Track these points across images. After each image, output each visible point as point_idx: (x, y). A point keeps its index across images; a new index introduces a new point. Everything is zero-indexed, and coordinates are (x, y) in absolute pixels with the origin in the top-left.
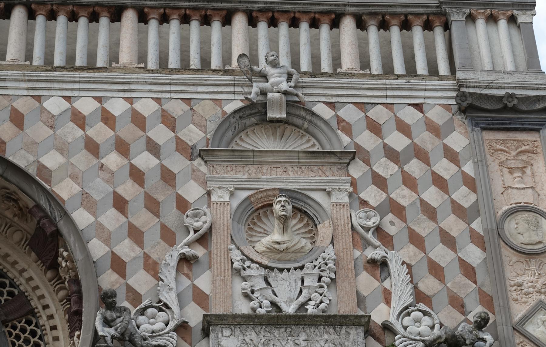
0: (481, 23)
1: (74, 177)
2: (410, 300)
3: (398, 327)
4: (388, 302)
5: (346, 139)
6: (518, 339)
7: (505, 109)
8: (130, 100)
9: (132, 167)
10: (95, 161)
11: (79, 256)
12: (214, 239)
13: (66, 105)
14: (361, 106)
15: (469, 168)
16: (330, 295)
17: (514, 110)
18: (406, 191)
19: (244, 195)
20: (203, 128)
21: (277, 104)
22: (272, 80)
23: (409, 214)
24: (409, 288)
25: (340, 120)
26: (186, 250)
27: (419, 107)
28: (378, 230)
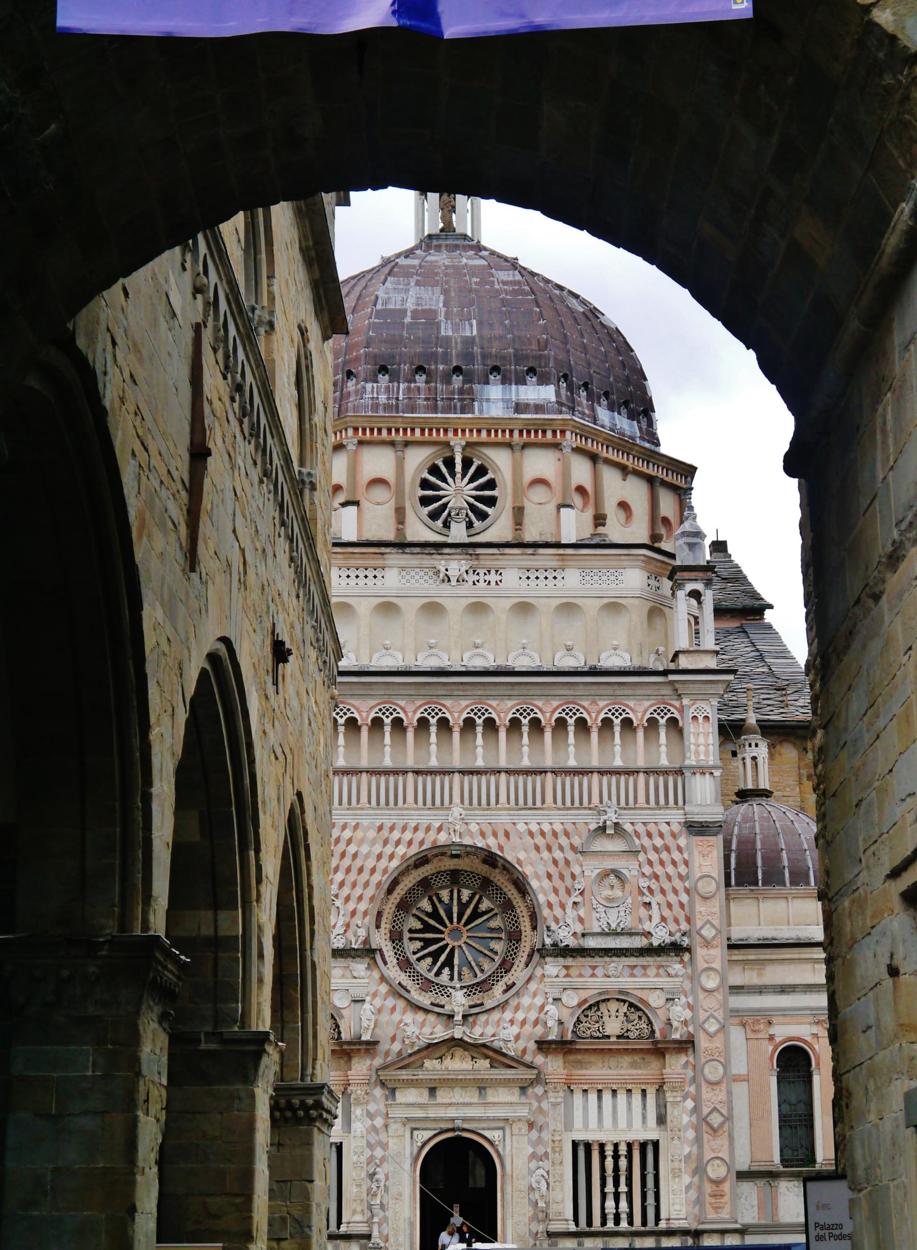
0: (698, 775)
1: (531, 864)
2: (659, 921)
3: (654, 934)
4: (650, 920)
5: (637, 842)
6: (698, 937)
7: (703, 826)
8: (551, 824)
9: (554, 858)
10: (539, 856)
11: (535, 902)
12: (585, 892)
13: (525, 827)
14: (644, 824)
15: (686, 856)
16: (629, 918)
17: (707, 827)
18: (660, 868)
19: (598, 871)
20: (580, 837)
21: (611, 827)
22: (609, 815)
23: (661, 879)
24: (659, 917)
25: (636, 832)
26: (576, 900)
27: (668, 823)
28: (649, 887)
